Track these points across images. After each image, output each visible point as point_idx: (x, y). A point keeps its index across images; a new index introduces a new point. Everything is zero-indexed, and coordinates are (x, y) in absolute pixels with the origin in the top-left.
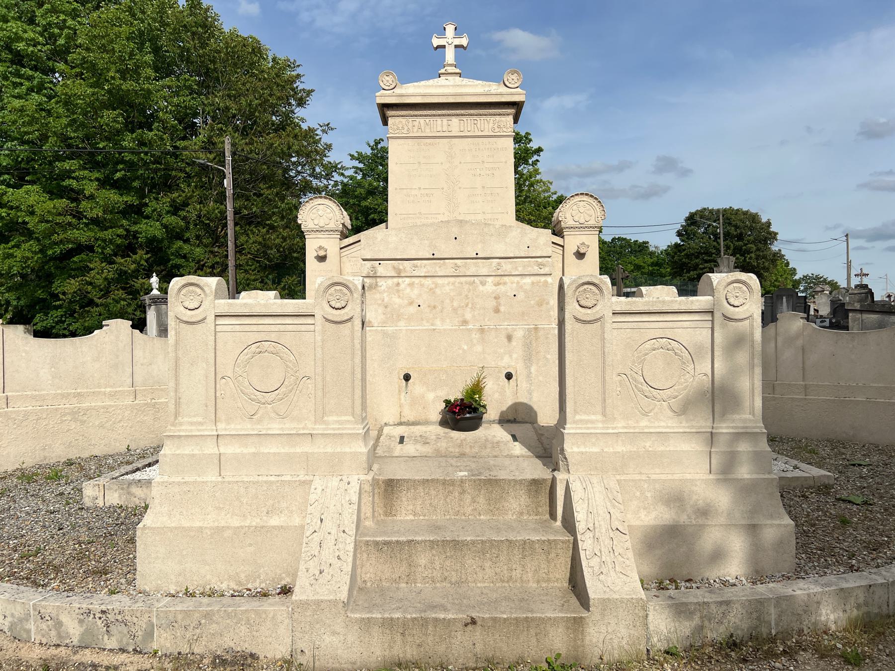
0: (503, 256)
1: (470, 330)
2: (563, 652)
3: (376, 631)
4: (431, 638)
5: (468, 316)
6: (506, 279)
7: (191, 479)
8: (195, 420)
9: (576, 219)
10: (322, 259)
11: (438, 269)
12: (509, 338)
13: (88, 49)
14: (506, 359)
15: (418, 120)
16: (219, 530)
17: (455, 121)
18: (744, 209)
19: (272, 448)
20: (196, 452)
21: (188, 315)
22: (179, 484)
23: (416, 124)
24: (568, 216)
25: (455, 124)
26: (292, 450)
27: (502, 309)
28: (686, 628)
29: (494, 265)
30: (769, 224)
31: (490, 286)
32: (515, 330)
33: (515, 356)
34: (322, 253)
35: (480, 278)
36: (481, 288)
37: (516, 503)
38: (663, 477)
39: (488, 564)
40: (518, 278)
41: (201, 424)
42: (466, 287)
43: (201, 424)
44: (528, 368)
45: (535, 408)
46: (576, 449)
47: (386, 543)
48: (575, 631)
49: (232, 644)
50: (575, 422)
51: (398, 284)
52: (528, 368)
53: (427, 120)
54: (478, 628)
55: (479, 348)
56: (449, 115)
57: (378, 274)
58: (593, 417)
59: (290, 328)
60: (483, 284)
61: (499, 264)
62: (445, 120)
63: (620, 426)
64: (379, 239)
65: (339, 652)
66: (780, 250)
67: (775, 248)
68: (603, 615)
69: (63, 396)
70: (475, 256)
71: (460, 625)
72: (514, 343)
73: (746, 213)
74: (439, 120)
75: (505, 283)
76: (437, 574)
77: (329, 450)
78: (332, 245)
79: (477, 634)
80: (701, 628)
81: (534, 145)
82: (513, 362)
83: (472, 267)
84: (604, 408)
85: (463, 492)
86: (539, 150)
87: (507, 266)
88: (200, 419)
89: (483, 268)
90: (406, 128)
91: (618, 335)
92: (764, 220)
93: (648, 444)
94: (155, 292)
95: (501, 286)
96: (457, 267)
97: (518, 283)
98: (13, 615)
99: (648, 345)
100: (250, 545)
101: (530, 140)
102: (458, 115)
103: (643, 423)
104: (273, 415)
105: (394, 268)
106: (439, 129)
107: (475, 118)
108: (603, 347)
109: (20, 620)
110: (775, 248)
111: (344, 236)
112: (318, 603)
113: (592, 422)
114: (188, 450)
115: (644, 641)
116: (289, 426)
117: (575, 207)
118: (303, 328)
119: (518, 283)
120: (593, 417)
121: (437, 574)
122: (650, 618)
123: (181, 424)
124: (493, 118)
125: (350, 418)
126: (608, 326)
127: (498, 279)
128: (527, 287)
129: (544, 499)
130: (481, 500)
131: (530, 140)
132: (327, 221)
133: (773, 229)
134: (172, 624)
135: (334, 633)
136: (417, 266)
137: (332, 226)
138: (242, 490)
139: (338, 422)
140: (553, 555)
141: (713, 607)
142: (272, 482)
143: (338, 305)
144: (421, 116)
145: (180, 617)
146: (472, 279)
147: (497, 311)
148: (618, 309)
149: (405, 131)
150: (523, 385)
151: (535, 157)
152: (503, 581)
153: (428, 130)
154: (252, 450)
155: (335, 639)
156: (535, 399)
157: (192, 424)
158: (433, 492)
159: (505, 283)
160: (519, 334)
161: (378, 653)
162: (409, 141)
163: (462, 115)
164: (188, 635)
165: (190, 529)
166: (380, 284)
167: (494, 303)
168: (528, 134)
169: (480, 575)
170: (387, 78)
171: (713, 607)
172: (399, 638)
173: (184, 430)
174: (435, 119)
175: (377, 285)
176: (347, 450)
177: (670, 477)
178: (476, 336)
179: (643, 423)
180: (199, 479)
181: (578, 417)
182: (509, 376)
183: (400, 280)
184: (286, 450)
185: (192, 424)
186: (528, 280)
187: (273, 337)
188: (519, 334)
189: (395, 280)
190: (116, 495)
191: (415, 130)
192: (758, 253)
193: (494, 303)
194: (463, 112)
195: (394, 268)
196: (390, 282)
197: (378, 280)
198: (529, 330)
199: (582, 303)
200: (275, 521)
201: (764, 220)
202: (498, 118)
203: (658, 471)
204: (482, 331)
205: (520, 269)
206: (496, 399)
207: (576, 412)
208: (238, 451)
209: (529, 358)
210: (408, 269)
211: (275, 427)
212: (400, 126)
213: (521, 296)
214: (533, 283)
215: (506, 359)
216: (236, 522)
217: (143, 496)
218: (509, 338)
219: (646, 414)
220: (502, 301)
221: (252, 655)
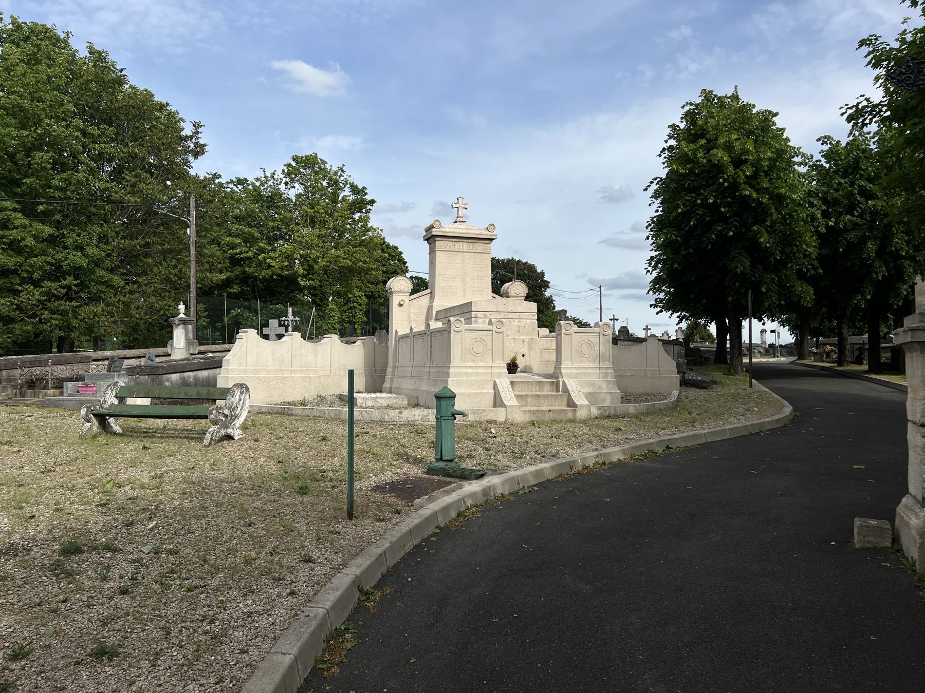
10: (401, 305)
13: (21, 96)
17: (466, 244)
18: (524, 261)
19: (480, 370)
25: (465, 246)
28: (599, 412)
30: (543, 274)
31: (516, 322)
63: (575, 365)
67: (547, 293)
69: (277, 370)
78: (406, 298)
79: (551, 413)
81: (368, 198)
82: (524, 350)
83: (511, 315)
86: (372, 202)
87: (522, 315)
91: (576, 339)
92: (539, 271)
94: (182, 316)
101: (366, 194)
103: (582, 365)
110: (547, 293)
111: (411, 294)
114: (458, 370)
129: (554, 387)
131: (366, 194)
137: (406, 290)
151: (369, 207)
168: (364, 188)
173: (456, 364)
179: (582, 365)
201: (539, 271)
206: (521, 362)
209: (530, 349)
211: (481, 364)
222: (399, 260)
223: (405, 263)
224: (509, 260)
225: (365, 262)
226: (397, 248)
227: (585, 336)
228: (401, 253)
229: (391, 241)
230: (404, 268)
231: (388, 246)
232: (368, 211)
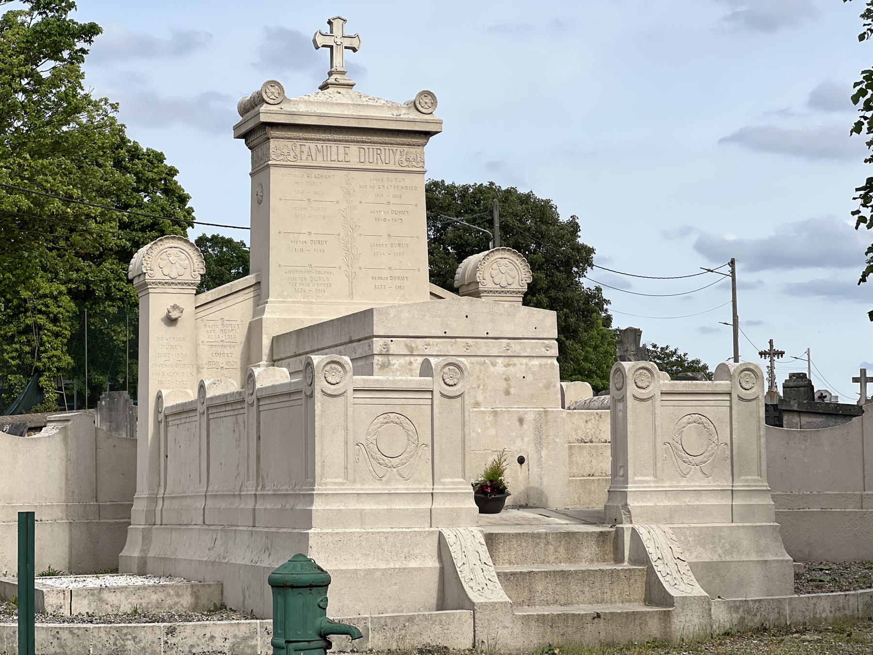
0: (512, 336)
1: (484, 413)
2: (658, 636)
3: (533, 624)
4: (570, 629)
5: (480, 398)
6: (515, 360)
7: (341, 530)
8: (337, 480)
9: (497, 280)
10: (171, 321)
11: (450, 348)
12: (521, 421)
14: (519, 442)
15: (308, 144)
16: (370, 572)
17: (354, 148)
18: (522, 190)
19: (399, 505)
20: (342, 508)
21: (330, 389)
22: (332, 534)
23: (305, 149)
24: (487, 276)
25: (353, 153)
26: (417, 507)
27: (512, 391)
28: (736, 617)
29: (504, 345)
30: (574, 227)
32: (526, 413)
33: (526, 439)
34: (174, 314)
35: (490, 358)
36: (492, 368)
37: (589, 550)
38: (700, 525)
39: (587, 589)
40: (525, 360)
41: (342, 484)
42: (477, 367)
43: (342, 484)
44: (539, 452)
45: (546, 491)
46: (636, 504)
47: (513, 574)
48: (665, 621)
49: (429, 641)
50: (635, 482)
51: (411, 363)
52: (539, 452)
53: (319, 146)
54: (602, 620)
55: (492, 431)
56: (347, 141)
57: (391, 352)
58: (647, 478)
59: (411, 401)
60: (494, 364)
61: (508, 345)
62: (341, 147)
63: (666, 485)
64: (392, 316)
65: (508, 641)
66: (599, 289)
67: (588, 281)
68: (683, 608)
70: (486, 335)
71: (589, 619)
72: (525, 427)
73: (526, 199)
74: (334, 146)
75: (514, 365)
76: (550, 598)
77: (448, 506)
78: (186, 301)
80: (742, 619)
82: (524, 445)
83: (483, 347)
84: (655, 470)
85: (548, 543)
86: (90, 31)
88: (341, 480)
89: (494, 348)
90: (292, 154)
91: (667, 412)
92: (564, 217)
93: (687, 500)
95: (511, 368)
96: (468, 346)
97: (527, 364)
98: (235, 636)
99: (685, 420)
100: (396, 584)
102: (358, 142)
103: (684, 484)
104: (398, 477)
105: (407, 345)
106: (334, 157)
107: (378, 146)
108: (654, 421)
109: (245, 639)
110: (588, 281)
112: (494, 604)
113: (647, 482)
114: (335, 505)
115: (709, 627)
116: (413, 487)
117: (495, 266)
118: (422, 402)
119: (527, 364)
120: (647, 478)
121: (550, 598)
122: (712, 610)
123: (326, 484)
124: (400, 148)
125: (462, 480)
126: (658, 403)
127: (507, 359)
128: (535, 369)
129: (609, 548)
130: (562, 550)
132: (181, 272)
133: (583, 239)
134: (383, 628)
135: (505, 627)
136: (428, 345)
137: (187, 277)
138: (383, 540)
139: (453, 483)
140: (632, 581)
141: (751, 603)
142: (406, 533)
143: (451, 383)
144: (312, 139)
145: (389, 621)
146: (483, 359)
147: (507, 393)
148: (664, 389)
149: (291, 158)
150: (534, 469)
151: (80, 45)
152: (598, 603)
153: (320, 158)
154: (386, 507)
155: (505, 631)
156: (544, 484)
157: (335, 484)
158: (524, 544)
159: (514, 365)
160: (530, 417)
161: (535, 642)
162: (297, 171)
163: (363, 142)
164: (396, 635)
165: (347, 571)
166: (392, 362)
167: (504, 385)
169: (581, 598)
170: (272, 89)
171: (751, 603)
172: (549, 630)
173: (330, 489)
174: (329, 144)
175: (389, 363)
176: (463, 506)
177: (704, 525)
178: (489, 418)
179: (684, 484)
180: (347, 530)
181: (636, 478)
182: (521, 460)
183: (412, 359)
184: (412, 507)
185: (335, 484)
186: (536, 362)
187: (398, 409)
188: (530, 417)
189: (407, 358)
190: (86, 602)
191: (304, 157)
192: (553, 293)
193: (504, 385)
194: (364, 138)
195: (407, 345)
196: (402, 360)
197: (390, 358)
198: (539, 413)
199: (640, 384)
200: (413, 564)
201: (564, 217)
202: (406, 149)
203: (695, 521)
204: (495, 413)
205: (528, 350)
206: (514, 480)
207: (635, 475)
208: (374, 507)
209: (539, 442)
210: (420, 347)
211: (401, 487)
212: (285, 151)
213: (530, 378)
214: (541, 365)
215: (519, 442)
216: (383, 566)
217: (116, 603)
218: (521, 421)
219: (684, 476)
220: (512, 383)
221: (446, 647)
222: (166, 191)
223: (183, 199)
224: (480, 189)
225: (68, 199)
226: (160, 157)
227: (690, 405)
228: (172, 172)
229: (142, 136)
230: (180, 214)
231: (135, 153)
232: (78, 57)
